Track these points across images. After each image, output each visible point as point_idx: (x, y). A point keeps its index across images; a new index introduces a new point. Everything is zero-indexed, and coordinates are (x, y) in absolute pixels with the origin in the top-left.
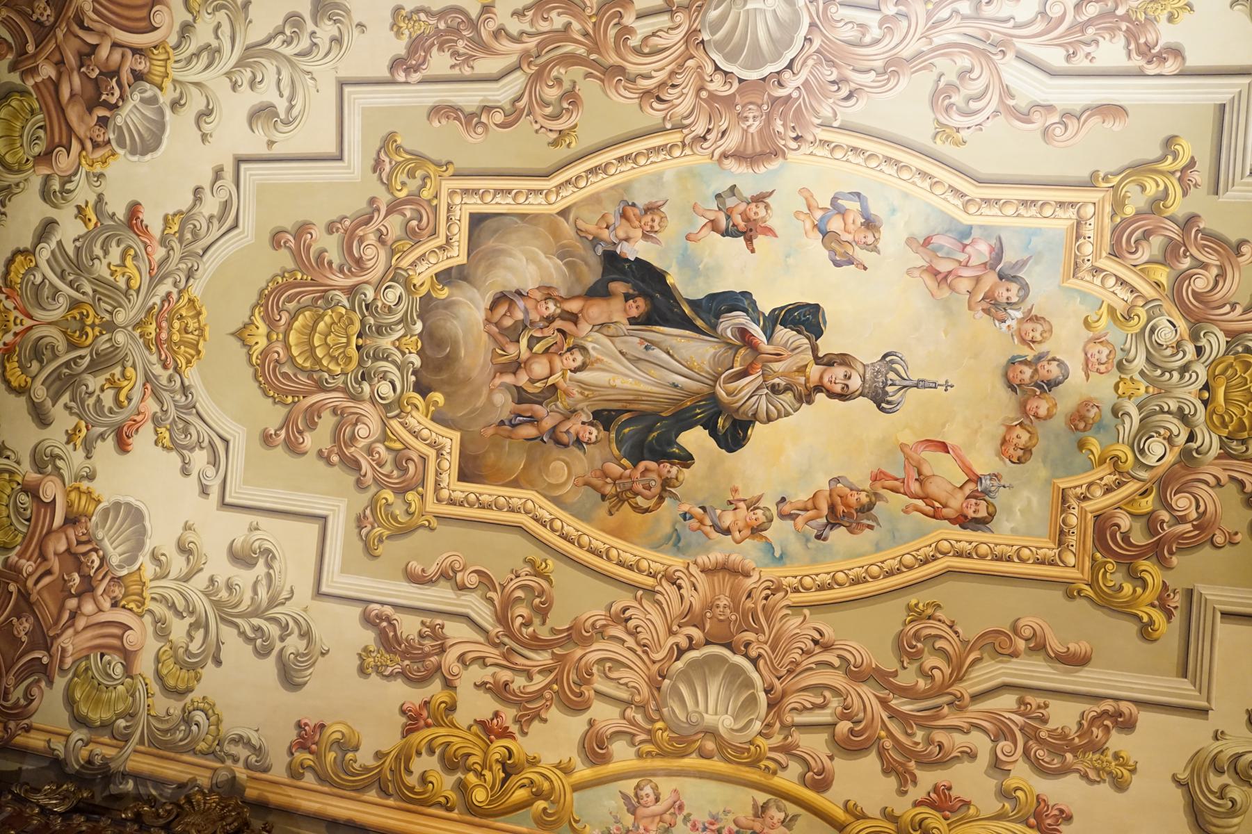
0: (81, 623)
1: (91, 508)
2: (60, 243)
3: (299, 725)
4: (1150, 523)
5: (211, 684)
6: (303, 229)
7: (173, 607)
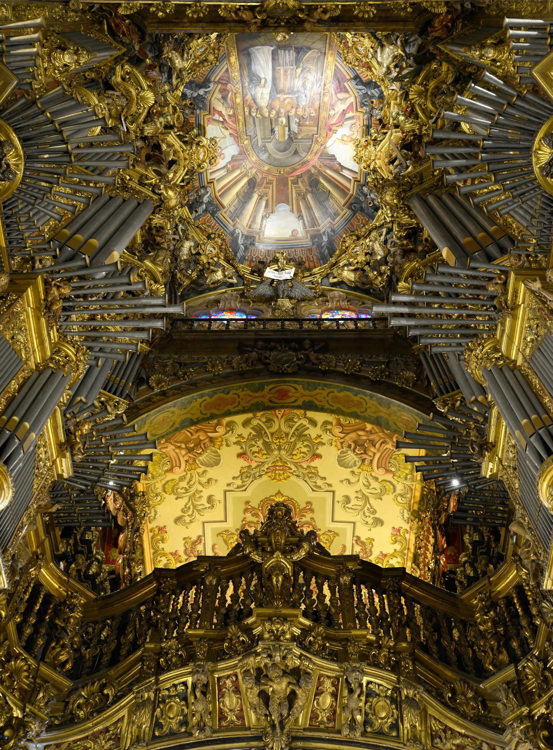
0: (178, 451)
1: (217, 446)
2: (308, 428)
3: (165, 527)
5: (170, 498)
6: (312, 511)
7: (190, 481)
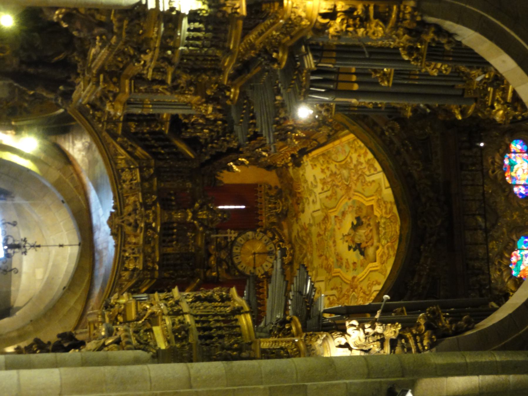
4: (326, 223)
